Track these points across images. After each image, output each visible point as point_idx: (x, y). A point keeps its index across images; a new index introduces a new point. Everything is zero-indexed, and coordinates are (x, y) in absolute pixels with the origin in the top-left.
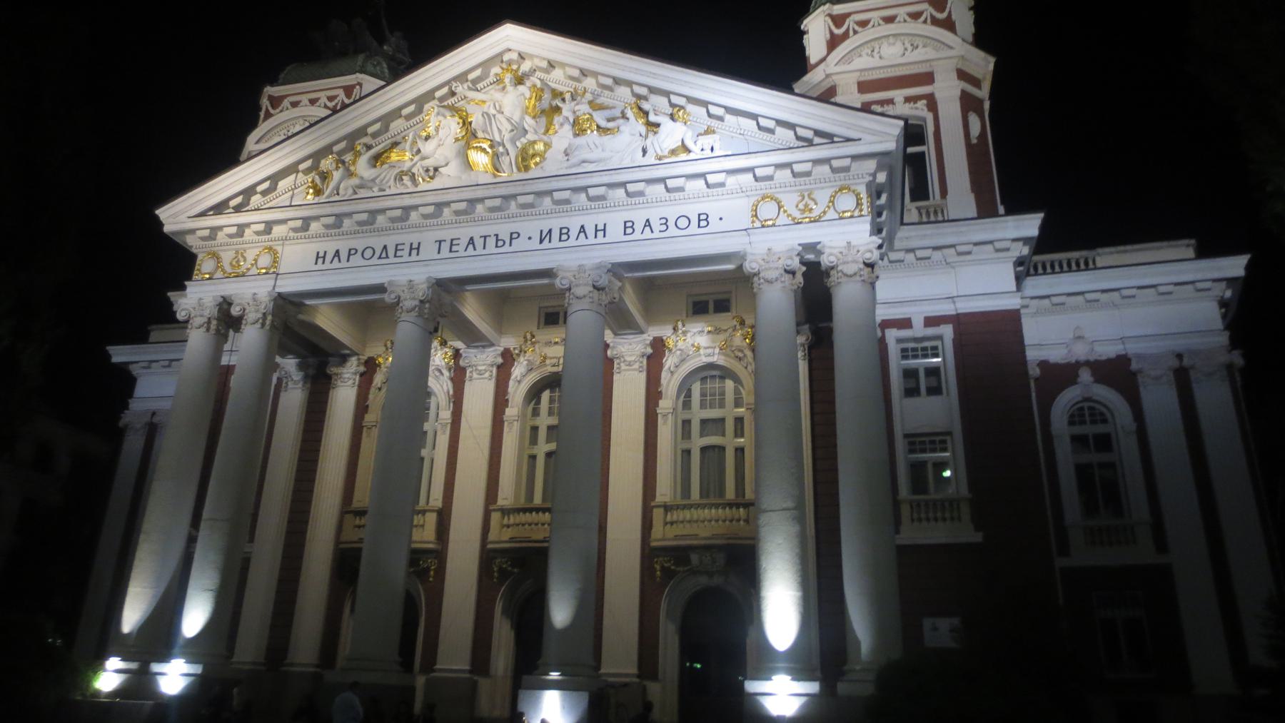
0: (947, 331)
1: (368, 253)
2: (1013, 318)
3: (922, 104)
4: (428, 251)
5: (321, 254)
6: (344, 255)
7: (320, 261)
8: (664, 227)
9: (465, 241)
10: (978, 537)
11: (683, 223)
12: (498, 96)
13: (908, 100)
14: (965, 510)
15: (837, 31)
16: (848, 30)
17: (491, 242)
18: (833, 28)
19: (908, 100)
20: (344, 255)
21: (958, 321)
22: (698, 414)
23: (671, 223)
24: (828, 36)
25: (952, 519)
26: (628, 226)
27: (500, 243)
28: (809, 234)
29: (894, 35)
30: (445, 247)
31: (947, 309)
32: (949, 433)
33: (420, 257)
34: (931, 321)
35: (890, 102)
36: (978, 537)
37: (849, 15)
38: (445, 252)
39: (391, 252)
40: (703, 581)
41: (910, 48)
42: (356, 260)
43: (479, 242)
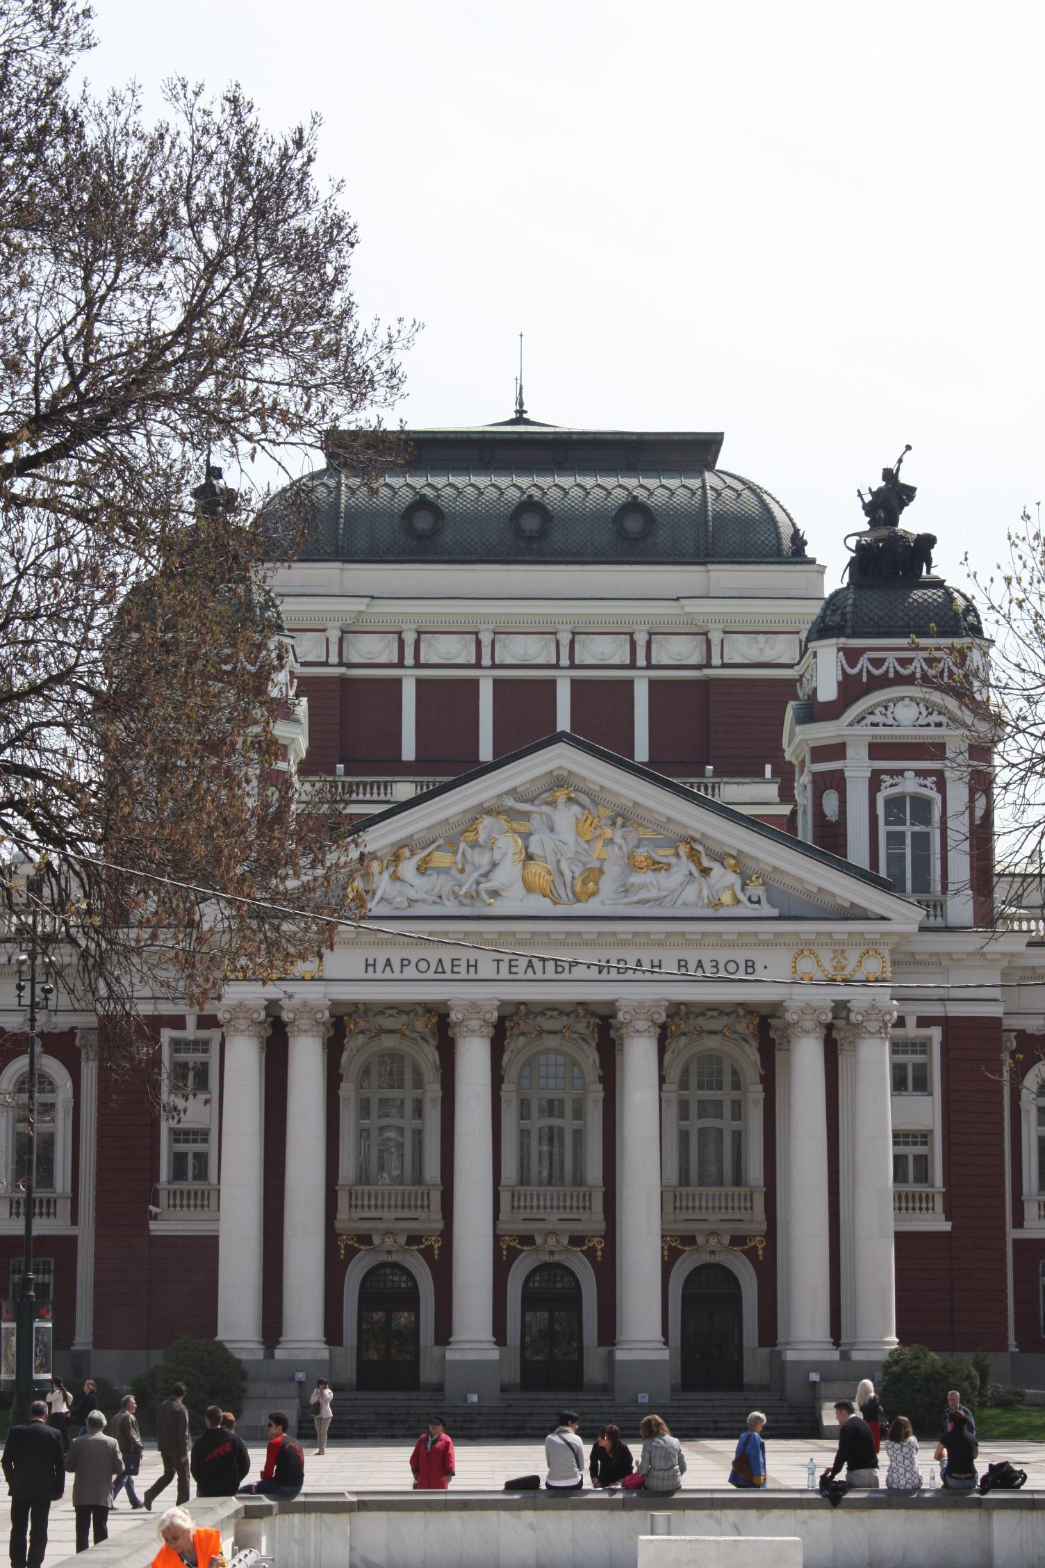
0: (936, 1033)
1: (423, 966)
2: (993, 1024)
3: (930, 781)
4: (487, 970)
5: (371, 962)
6: (396, 965)
7: (371, 969)
8: (715, 970)
9: (523, 963)
10: (947, 1226)
11: (732, 967)
12: (546, 809)
13: (919, 773)
14: (939, 1203)
15: (849, 671)
16: (861, 670)
17: (550, 966)
18: (846, 666)
19: (919, 773)
20: (396, 965)
21: (946, 1023)
22: (727, 1124)
23: (721, 966)
24: (840, 678)
25: (927, 1209)
26: (682, 964)
27: (560, 969)
28: (841, 993)
29: (911, 699)
30: (504, 967)
31: (936, 1010)
32: (931, 1131)
33: (480, 976)
34: (924, 1022)
35: (900, 773)
36: (947, 1226)
37: (862, 651)
38: (504, 974)
39: (448, 967)
40: (706, 1258)
41: (925, 713)
42: (410, 972)
43: (538, 965)
